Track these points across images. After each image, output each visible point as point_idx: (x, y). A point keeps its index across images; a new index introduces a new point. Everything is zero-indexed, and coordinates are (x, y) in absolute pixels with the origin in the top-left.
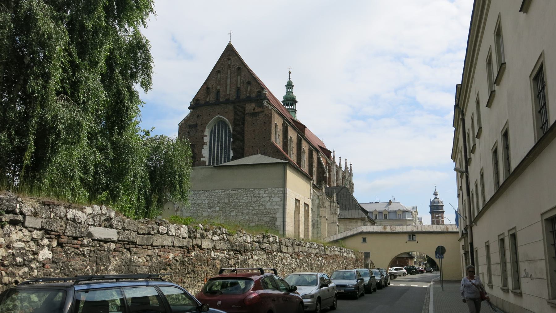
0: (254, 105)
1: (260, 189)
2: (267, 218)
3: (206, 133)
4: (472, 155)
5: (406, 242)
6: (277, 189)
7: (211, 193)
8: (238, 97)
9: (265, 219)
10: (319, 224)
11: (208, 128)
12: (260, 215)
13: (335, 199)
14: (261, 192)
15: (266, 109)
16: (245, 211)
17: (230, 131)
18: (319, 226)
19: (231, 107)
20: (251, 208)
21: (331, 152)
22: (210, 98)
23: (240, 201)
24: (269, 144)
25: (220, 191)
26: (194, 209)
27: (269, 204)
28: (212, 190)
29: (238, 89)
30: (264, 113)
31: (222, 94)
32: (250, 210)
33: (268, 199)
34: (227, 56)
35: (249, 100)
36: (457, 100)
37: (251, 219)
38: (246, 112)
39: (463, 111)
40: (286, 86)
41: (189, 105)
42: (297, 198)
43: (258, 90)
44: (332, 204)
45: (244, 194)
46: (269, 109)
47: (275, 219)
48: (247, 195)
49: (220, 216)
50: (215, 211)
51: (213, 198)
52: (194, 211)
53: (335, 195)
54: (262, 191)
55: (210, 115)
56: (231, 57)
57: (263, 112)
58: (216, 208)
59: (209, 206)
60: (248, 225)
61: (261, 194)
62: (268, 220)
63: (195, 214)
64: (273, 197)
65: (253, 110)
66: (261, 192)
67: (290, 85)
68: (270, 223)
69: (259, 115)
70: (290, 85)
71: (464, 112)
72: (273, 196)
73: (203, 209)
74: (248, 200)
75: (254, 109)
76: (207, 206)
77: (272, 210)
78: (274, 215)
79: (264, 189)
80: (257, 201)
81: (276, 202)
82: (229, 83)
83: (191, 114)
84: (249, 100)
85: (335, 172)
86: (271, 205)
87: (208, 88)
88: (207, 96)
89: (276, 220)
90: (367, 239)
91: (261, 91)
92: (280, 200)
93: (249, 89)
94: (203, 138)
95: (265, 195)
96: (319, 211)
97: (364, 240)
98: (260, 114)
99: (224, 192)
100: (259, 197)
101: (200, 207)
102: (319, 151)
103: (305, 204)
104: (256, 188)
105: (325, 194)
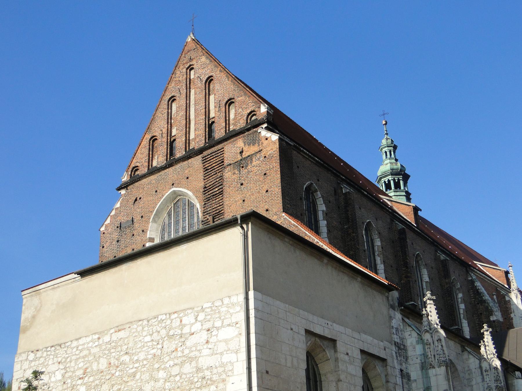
0: (240, 143)
11: (154, 221)
14: (185, 320)
17: (198, 216)
19: (197, 162)
20: (162, 374)
22: (158, 158)
23: (136, 358)
25: (89, 339)
28: (71, 341)
30: (262, 154)
33: (204, 335)
34: (188, 62)
38: (226, 163)
42: (318, 330)
43: (249, 111)
45: (145, 333)
51: (73, 364)
56: (194, 62)
61: (185, 325)
64: (218, 329)
69: (251, 163)
75: (241, 152)
79: (192, 309)
80: (176, 350)
81: (226, 341)
91: (256, 109)
93: (232, 116)
95: (197, 327)
96: (427, 377)
98: (254, 159)
99: (99, 338)
103: (363, 352)
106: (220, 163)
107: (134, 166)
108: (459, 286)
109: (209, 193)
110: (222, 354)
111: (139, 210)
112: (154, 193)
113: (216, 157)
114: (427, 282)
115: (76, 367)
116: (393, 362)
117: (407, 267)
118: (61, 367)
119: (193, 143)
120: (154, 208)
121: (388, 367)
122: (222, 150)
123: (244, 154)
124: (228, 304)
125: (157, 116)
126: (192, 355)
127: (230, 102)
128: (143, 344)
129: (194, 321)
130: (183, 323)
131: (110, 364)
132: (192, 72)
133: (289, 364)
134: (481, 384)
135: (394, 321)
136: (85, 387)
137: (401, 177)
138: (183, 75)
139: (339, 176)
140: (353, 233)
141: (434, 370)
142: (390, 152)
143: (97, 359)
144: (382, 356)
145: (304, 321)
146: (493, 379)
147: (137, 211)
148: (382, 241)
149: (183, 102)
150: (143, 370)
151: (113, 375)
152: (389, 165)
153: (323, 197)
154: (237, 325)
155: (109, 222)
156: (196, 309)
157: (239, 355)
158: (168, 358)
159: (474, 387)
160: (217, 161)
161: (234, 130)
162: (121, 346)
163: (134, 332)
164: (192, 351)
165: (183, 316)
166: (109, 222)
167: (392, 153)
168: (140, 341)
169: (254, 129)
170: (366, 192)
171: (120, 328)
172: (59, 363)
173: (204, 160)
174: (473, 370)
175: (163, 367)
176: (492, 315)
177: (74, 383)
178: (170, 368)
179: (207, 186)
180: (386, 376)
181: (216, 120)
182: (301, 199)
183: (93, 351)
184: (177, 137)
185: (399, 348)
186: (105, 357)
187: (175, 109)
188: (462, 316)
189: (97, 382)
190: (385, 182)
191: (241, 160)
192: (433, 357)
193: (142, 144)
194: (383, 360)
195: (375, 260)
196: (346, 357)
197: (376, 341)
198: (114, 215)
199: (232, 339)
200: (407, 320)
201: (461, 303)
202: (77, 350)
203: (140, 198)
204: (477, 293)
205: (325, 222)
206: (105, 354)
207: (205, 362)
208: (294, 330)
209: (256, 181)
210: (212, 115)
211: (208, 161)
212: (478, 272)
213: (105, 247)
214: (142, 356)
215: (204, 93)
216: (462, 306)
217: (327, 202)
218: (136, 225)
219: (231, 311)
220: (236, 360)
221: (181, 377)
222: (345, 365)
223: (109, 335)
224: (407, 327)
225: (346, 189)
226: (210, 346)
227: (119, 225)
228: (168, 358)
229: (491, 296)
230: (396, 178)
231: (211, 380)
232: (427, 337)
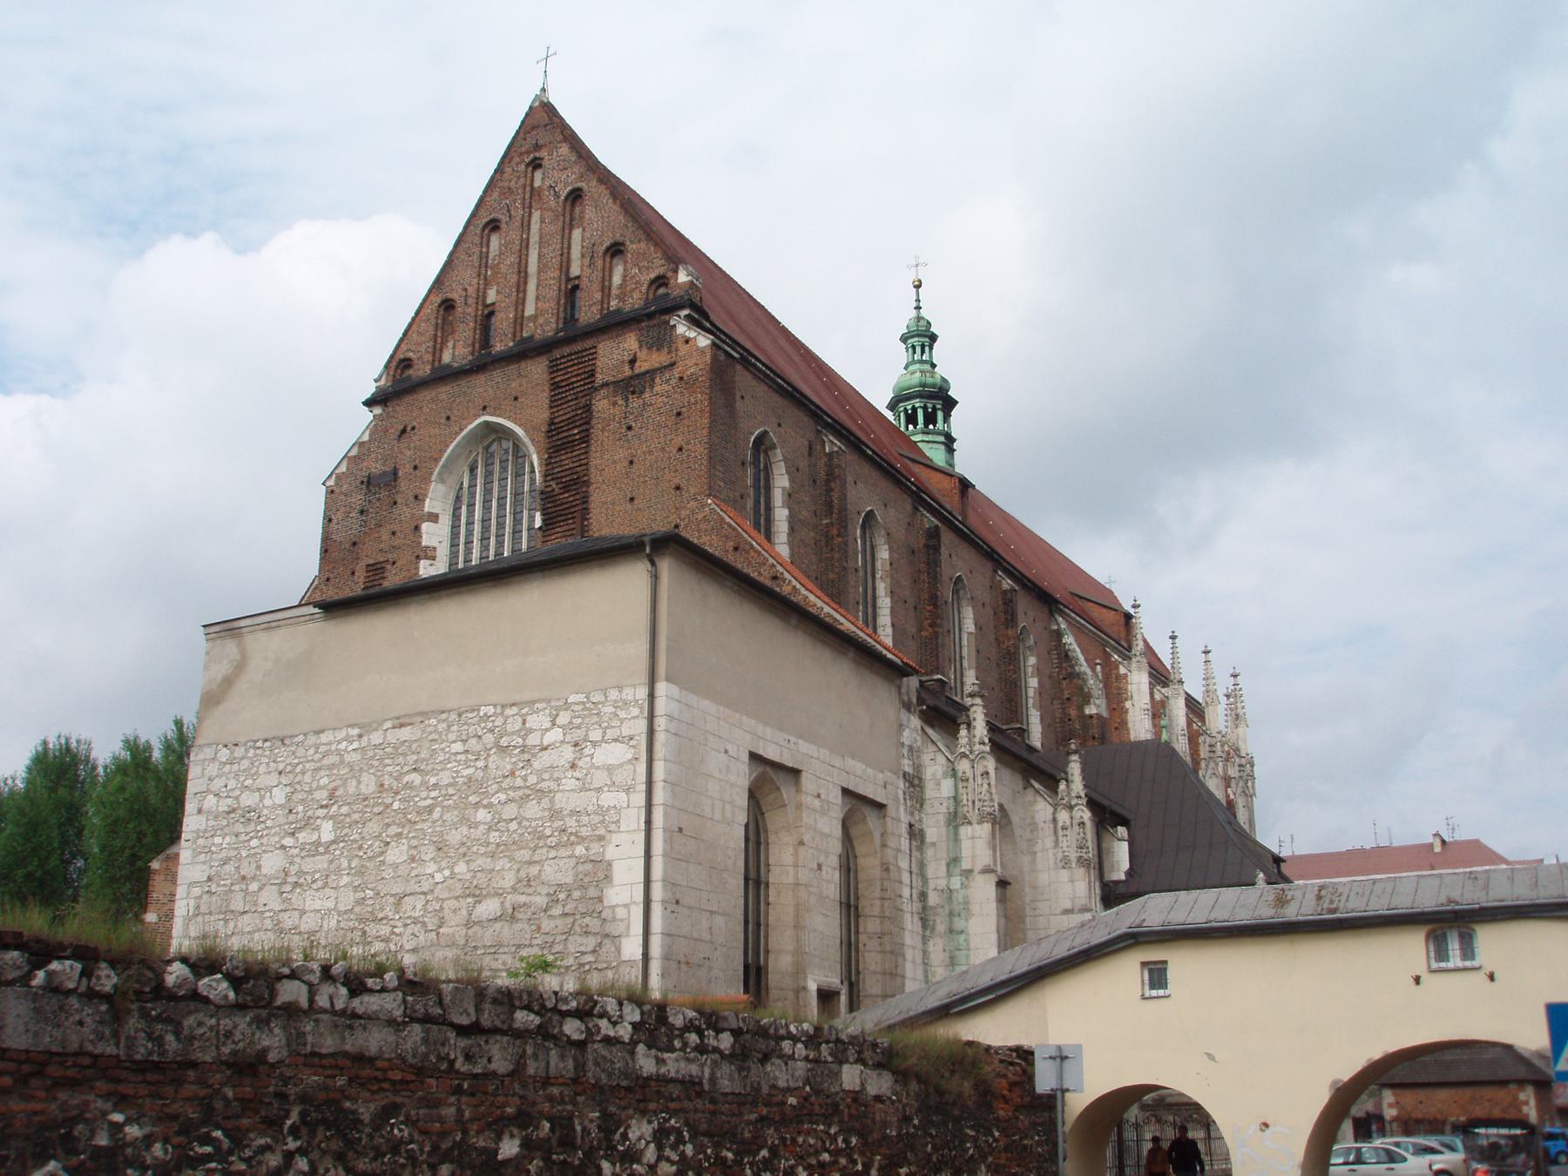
0: (630, 342)
1: (533, 702)
2: (558, 871)
3: (429, 506)
5: (1417, 980)
7: (300, 752)
8: (570, 318)
10: (957, 908)
11: (442, 480)
12: (524, 854)
13: (1078, 786)
14: (533, 721)
16: (455, 837)
17: (533, 480)
18: (959, 924)
19: (537, 370)
20: (482, 815)
21: (1128, 617)
22: (454, 348)
23: (433, 780)
25: (343, 734)
26: (228, 839)
28: (305, 735)
29: (572, 291)
30: (676, 372)
31: (502, 323)
32: (476, 825)
33: (568, 753)
34: (528, 153)
35: (614, 324)
37: (481, 879)
38: (600, 378)
40: (904, 339)
41: (370, 390)
42: (771, 753)
43: (653, 276)
44: (1063, 816)
45: (452, 737)
46: (698, 349)
47: (600, 872)
49: (339, 869)
50: (318, 843)
51: (307, 778)
52: (224, 854)
53: (1075, 768)
55: (448, 418)
56: (544, 153)
57: (673, 365)
58: (317, 829)
59: (292, 818)
60: (464, 912)
61: (531, 731)
62: (568, 879)
63: (227, 868)
64: (594, 744)
65: (627, 368)
66: (537, 720)
67: (922, 337)
68: (576, 894)
69: (652, 387)
70: (922, 337)
73: (265, 841)
74: (466, 772)
75: (633, 362)
76: (282, 820)
77: (585, 819)
78: (595, 848)
79: (548, 701)
80: (512, 774)
81: (610, 769)
82: (533, 268)
83: (377, 429)
84: (614, 324)
86: (583, 789)
87: (448, 306)
88: (443, 344)
89: (608, 878)
90: (1171, 974)
91: (670, 274)
93: (617, 279)
94: (417, 528)
95: (554, 735)
97: (1157, 976)
98: (658, 380)
99: (360, 736)
101: (252, 827)
102: (1056, 602)
103: (846, 792)
105: (987, 748)
106: (586, 378)
107: (402, 357)
108: (1032, 642)
109: (560, 436)
111: (408, 453)
112: (443, 421)
113: (579, 363)
114: (970, 634)
115: (314, 786)
116: (898, 808)
117: (935, 606)
118: (284, 780)
119: (531, 324)
120: (442, 452)
121: (888, 819)
122: (591, 351)
123: (637, 364)
124: (616, 701)
125: (457, 258)
126: (543, 785)
127: (616, 250)
128: (448, 755)
129: (549, 725)
131: (382, 785)
132: (538, 175)
133: (718, 816)
134: (1051, 852)
135: (906, 733)
136: (331, 822)
138: (519, 178)
139: (823, 419)
140: (838, 536)
141: (969, 828)
142: (923, 347)
143: (355, 772)
144: (879, 799)
145: (748, 737)
146: (1074, 844)
147: (406, 456)
148: (891, 550)
149: (514, 236)
150: (445, 803)
151: (387, 807)
153: (785, 460)
154: (632, 743)
155: (344, 470)
156: (553, 703)
157: (632, 797)
159: (1039, 854)
160: (580, 372)
161: (618, 311)
162: (404, 755)
163: (431, 733)
164: (544, 780)
165: (527, 714)
166: (344, 470)
167: (927, 349)
168: (443, 749)
169: (663, 317)
170: (870, 449)
171: (401, 720)
172: (280, 773)
173: (553, 368)
174: (1041, 825)
175: (485, 802)
176: (1088, 703)
177: (310, 813)
178: (499, 807)
179: (556, 421)
180: (882, 835)
181: (584, 283)
182: (743, 464)
183: (347, 758)
184: (497, 308)
185: (912, 784)
186: (372, 771)
187: (497, 248)
188: (1031, 701)
189: (356, 816)
190: (906, 410)
191: (631, 378)
192: (970, 803)
193: (422, 314)
194: (880, 807)
195: (874, 589)
196: (817, 802)
197: (870, 771)
198: (355, 457)
199: (621, 765)
200: (930, 731)
201: (1032, 677)
202: (316, 752)
203: (413, 428)
204: (1065, 656)
205: (786, 512)
206: (373, 766)
208: (730, 753)
209: (659, 425)
210: (575, 270)
211: (561, 369)
212: (1073, 615)
213: (335, 521)
214: (445, 778)
215: (560, 223)
216: (1033, 682)
217: (793, 471)
218: (403, 484)
219: (622, 714)
220: (625, 805)
221: (519, 823)
222: (813, 817)
223: (381, 732)
224: (930, 744)
225: (832, 444)
226: (577, 774)
227: (365, 480)
229: (1093, 667)
230: (930, 405)
231: (577, 836)
232: (963, 766)
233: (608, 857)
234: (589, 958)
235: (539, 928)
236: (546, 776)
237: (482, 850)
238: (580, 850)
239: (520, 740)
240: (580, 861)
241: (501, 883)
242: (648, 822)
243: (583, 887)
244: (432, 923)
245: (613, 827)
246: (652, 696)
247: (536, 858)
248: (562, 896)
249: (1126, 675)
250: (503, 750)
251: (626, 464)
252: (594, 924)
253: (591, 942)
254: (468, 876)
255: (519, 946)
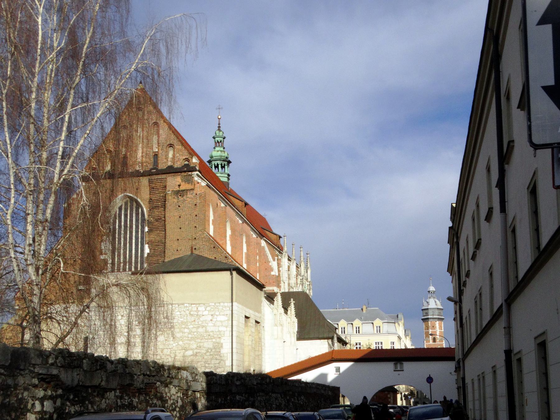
2: (208, 344)
4: (467, 279)
6: (222, 304)
9: (206, 345)
12: (199, 341)
14: (200, 309)
15: (197, 185)
20: (186, 330)
24: (203, 237)
27: (212, 325)
30: (195, 192)
32: (185, 333)
33: (210, 318)
35: (171, 171)
36: (452, 216)
37: (187, 346)
39: (457, 233)
42: (247, 315)
43: (184, 158)
48: (180, 312)
54: (201, 307)
57: (193, 189)
60: (182, 353)
62: (211, 346)
64: (217, 315)
66: (201, 308)
69: (187, 195)
71: (459, 235)
72: (217, 313)
74: (182, 319)
75: (179, 186)
78: (218, 340)
79: (204, 304)
81: (221, 322)
84: (171, 171)
85: (286, 267)
86: (215, 326)
89: (222, 347)
91: (190, 159)
92: (227, 319)
95: (206, 313)
98: (188, 193)
100: (197, 315)
104: (193, 303)
110: (219, 326)
123: (181, 187)
126: (203, 324)
129: (204, 310)
130: (198, 309)
137: (226, 163)
152: (220, 152)
158: (190, 324)
173: (150, 182)
179: (153, 199)
181: (160, 155)
199: (224, 321)
207: (210, 329)
226: (212, 322)
228: (190, 324)
230: (223, 164)
233: (222, 342)
234: (217, 365)
235: (203, 358)
236: (204, 322)
237: (187, 339)
238: (214, 340)
239: (196, 313)
240: (214, 343)
241: (193, 347)
242: (232, 335)
243: (215, 349)
244: (173, 356)
245: (222, 335)
246: (232, 306)
247: (202, 341)
248: (210, 351)
249: (280, 259)
250: (192, 315)
251: (178, 217)
252: (218, 357)
253: (218, 361)
254: (183, 345)
255: (198, 362)
